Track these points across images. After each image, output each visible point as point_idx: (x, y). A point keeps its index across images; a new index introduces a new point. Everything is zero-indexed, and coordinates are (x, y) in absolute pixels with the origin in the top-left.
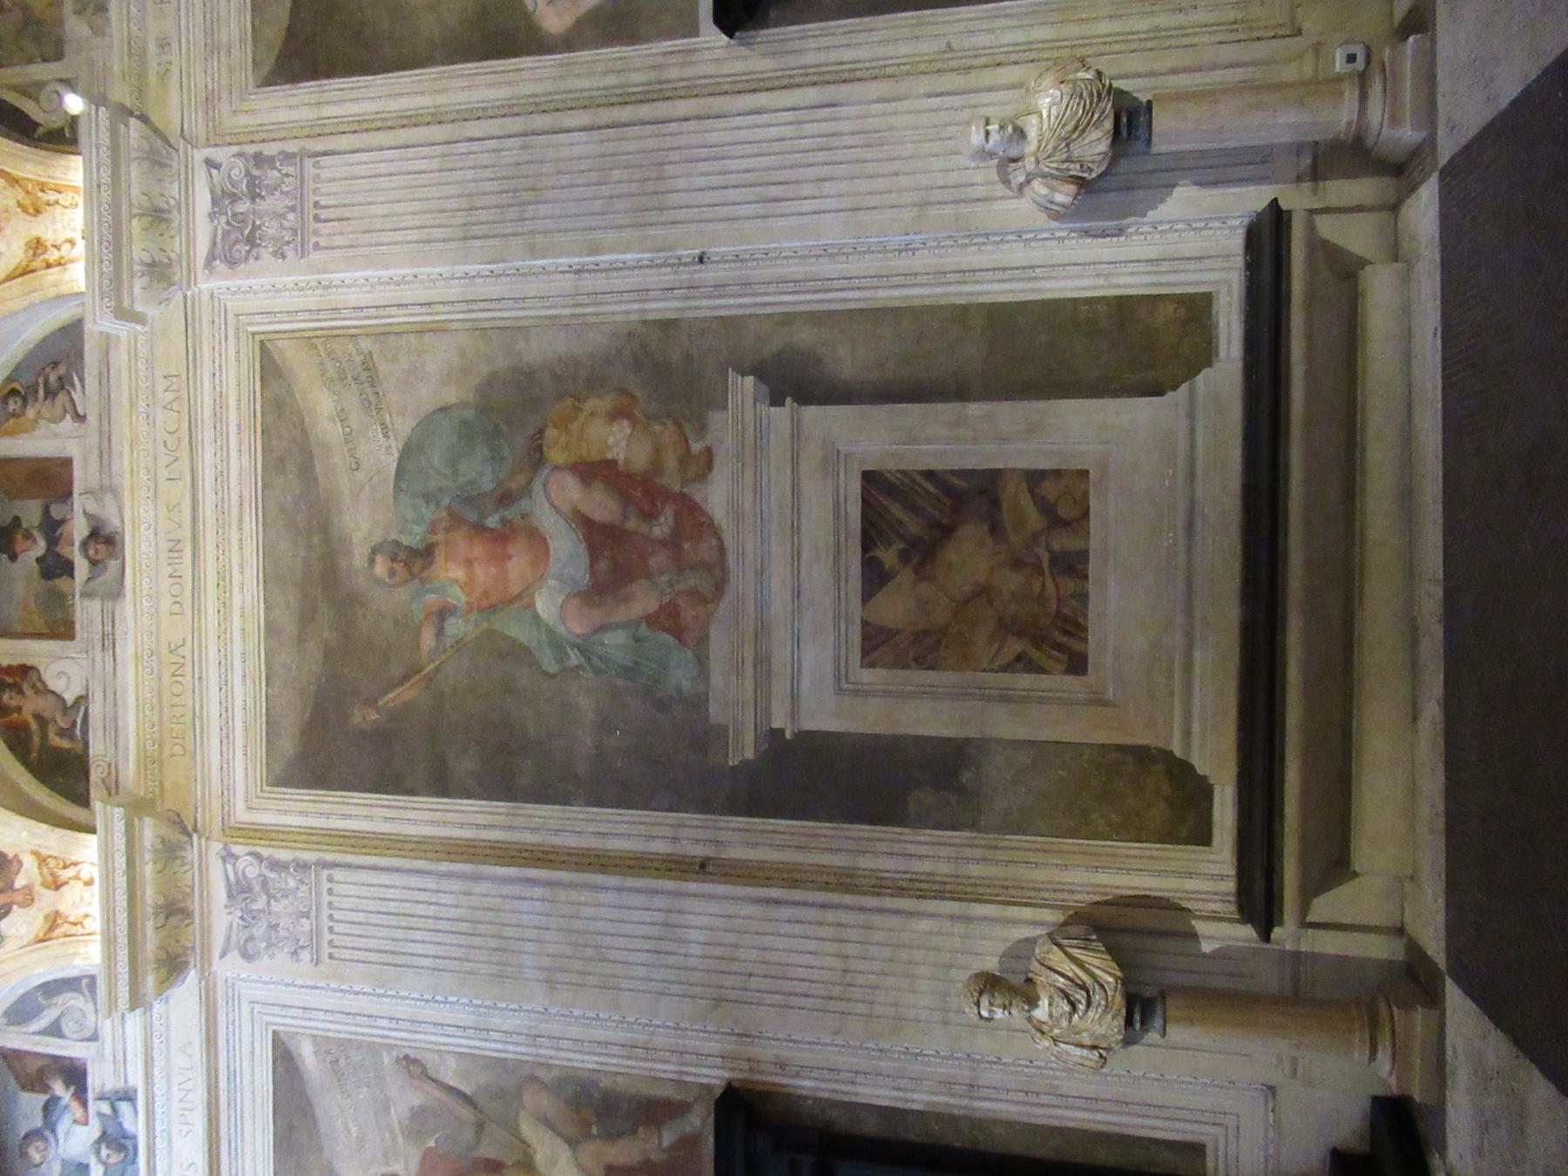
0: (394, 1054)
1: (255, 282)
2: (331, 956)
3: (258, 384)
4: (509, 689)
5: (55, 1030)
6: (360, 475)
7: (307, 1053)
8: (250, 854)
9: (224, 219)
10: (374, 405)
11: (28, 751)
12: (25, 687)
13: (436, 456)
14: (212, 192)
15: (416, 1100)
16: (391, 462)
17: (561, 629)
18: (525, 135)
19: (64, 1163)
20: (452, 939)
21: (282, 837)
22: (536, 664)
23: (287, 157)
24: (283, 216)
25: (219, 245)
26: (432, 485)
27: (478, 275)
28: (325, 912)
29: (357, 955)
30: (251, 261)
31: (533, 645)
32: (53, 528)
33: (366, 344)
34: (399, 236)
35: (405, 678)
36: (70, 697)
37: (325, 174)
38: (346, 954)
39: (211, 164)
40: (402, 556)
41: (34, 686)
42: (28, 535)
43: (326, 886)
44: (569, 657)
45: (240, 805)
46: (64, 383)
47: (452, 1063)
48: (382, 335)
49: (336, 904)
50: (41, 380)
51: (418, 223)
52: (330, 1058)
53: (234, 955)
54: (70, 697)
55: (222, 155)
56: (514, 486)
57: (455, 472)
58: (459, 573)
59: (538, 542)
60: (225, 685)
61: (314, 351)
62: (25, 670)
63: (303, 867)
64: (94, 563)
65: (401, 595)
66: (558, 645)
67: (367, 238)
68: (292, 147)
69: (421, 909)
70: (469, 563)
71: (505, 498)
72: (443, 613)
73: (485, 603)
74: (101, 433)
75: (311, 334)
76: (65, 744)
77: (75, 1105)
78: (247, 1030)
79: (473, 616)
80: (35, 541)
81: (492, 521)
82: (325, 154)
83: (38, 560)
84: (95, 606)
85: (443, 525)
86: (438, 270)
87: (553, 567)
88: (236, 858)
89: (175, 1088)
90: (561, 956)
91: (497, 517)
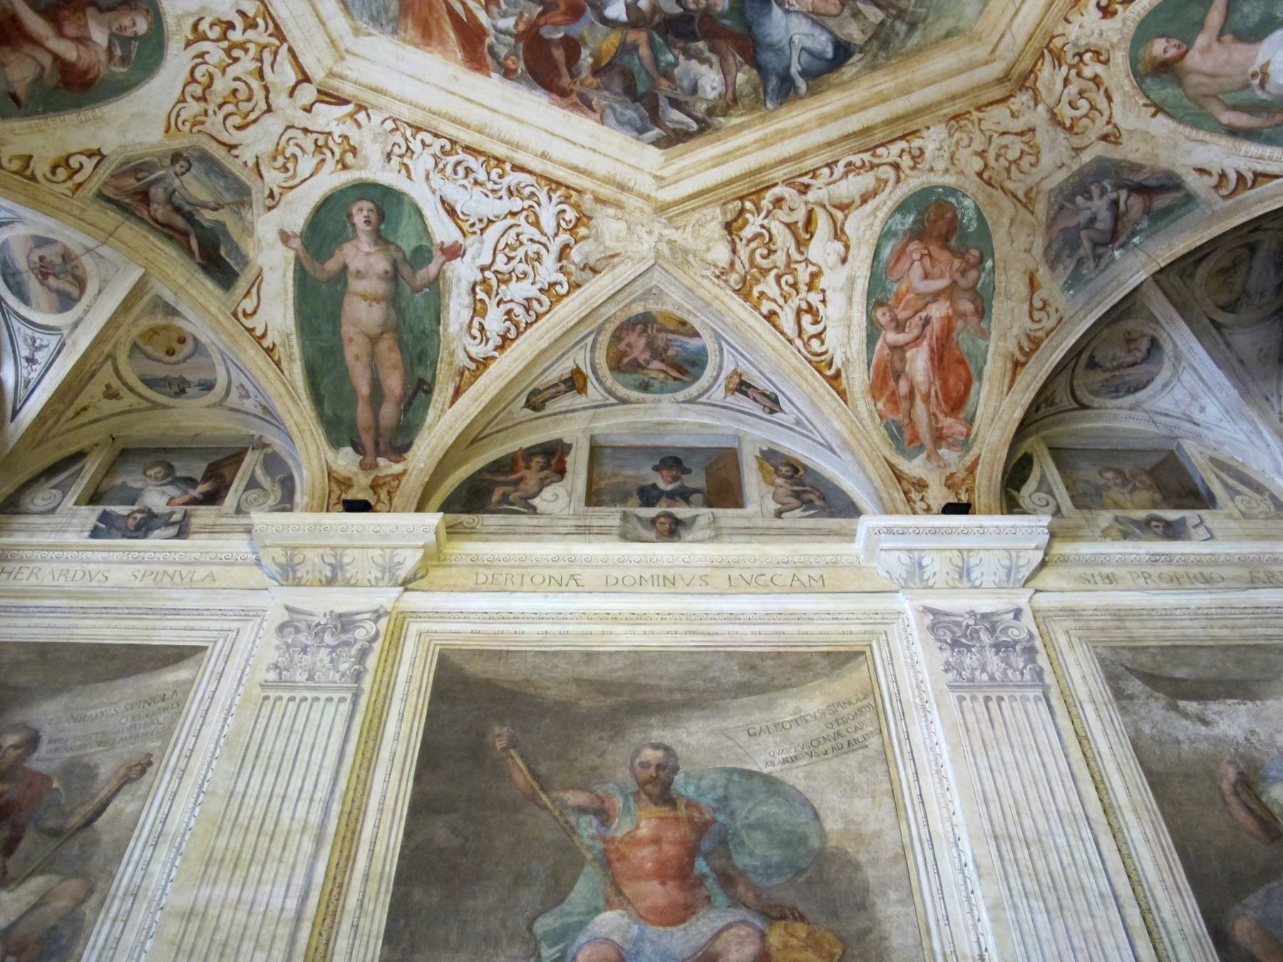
0: (157, 752)
1: (918, 647)
2: (266, 698)
3: (825, 649)
4: (520, 879)
5: (252, 484)
6: (743, 737)
7: (181, 674)
8: (377, 633)
9: (971, 622)
10: (813, 749)
11: (490, 472)
12: (546, 472)
13: (768, 809)
14: (992, 614)
15: (105, 772)
16: (759, 766)
17: (582, 939)
18: (1116, 898)
19: (141, 490)
20: (259, 811)
21: (390, 660)
22: (541, 913)
23: (1039, 673)
24: (984, 670)
25: (946, 619)
26: (737, 804)
27: (959, 852)
28: (310, 695)
29: (262, 722)
30: (939, 644)
31: (566, 907)
32: (684, 495)
33: (874, 742)
34: (985, 773)
35: (536, 776)
36: (536, 502)
37: (1031, 706)
38: (265, 712)
39: (1018, 613)
40: (662, 774)
41: (546, 478)
42: (675, 479)
43: (336, 696)
44: (550, 947)
45: (425, 626)
46: (809, 504)
47: (131, 808)
48: (885, 756)
49: (316, 704)
50: (808, 488)
51: (1002, 790)
52: (169, 693)
53: (286, 616)
54: (536, 502)
55: (1027, 619)
56: (741, 889)
57: (750, 827)
58: (644, 831)
59: (678, 915)
60: (539, 617)
61: (861, 696)
62: (561, 472)
63: (358, 677)
64: (653, 521)
65: (623, 774)
66: (565, 934)
67: (978, 743)
68: (1049, 678)
69: (296, 783)
70: (656, 841)
71: (727, 879)
72: (603, 814)
73: (613, 856)
74: (767, 528)
75: (877, 695)
77: (186, 498)
78: (218, 625)
79: (599, 845)
80: (670, 483)
81: (701, 865)
82: (1050, 707)
83: (654, 486)
84: (617, 522)
85: (696, 815)
86: (959, 812)
87: (652, 931)
88: (376, 621)
89: (178, 568)
90: (216, 928)
91: (706, 870)
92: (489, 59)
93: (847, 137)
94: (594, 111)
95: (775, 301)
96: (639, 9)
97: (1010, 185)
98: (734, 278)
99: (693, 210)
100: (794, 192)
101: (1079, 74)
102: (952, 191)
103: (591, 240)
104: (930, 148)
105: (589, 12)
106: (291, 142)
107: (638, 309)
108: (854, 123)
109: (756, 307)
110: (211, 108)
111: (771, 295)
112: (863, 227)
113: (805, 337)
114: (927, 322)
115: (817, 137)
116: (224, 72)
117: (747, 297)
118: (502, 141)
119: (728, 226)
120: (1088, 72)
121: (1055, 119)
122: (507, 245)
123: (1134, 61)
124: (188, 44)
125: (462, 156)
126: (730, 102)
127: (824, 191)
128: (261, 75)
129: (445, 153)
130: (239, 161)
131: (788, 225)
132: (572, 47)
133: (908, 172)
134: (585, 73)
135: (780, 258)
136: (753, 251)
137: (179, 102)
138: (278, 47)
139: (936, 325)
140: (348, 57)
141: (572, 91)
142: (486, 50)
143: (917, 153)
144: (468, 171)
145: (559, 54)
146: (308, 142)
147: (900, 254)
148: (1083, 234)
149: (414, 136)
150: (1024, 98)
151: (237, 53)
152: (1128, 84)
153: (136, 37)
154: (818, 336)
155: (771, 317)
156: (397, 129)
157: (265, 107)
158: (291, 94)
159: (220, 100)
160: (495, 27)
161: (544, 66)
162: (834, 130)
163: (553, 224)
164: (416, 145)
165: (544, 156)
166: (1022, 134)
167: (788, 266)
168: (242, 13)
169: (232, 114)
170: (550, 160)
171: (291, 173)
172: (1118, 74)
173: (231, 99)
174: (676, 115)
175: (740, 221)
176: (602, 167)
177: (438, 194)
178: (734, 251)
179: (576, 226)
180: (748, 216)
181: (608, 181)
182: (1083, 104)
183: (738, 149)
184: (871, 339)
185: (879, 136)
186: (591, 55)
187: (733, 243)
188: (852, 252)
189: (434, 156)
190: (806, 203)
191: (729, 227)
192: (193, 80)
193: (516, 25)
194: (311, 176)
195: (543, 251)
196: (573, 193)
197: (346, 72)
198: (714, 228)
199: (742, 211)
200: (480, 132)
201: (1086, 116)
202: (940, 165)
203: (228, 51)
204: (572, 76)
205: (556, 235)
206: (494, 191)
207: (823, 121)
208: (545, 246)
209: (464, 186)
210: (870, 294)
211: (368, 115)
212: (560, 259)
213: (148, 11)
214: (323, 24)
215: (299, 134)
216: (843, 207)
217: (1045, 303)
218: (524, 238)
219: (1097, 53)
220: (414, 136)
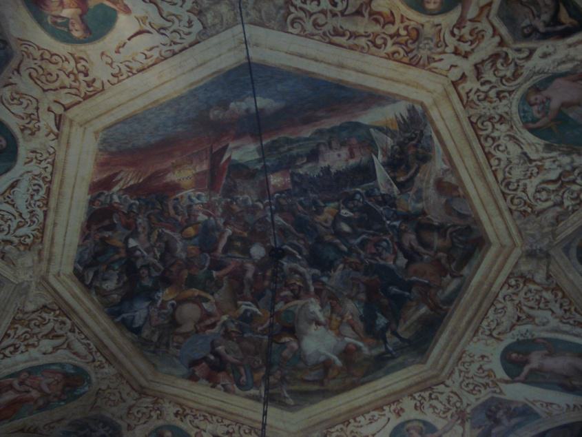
92: (97, 193)
93: (101, 341)
94: (85, 239)
95: (15, 334)
96: (135, 251)
97: (99, 400)
98: (20, 315)
99: (48, 291)
100: (70, 327)
101: (151, 411)
102: (90, 382)
103: (18, 252)
104: (106, 370)
105: (130, 232)
106: (29, 102)
108: (107, 341)
109: (9, 328)
110: (39, 63)
111: (18, 332)
112: (63, 356)
113: (3, 351)
114: (28, 392)
115: (97, 329)
116: (60, 70)
117: (12, 323)
118: (57, 205)
119: (45, 307)
120: (152, 414)
121: (130, 408)
122: (3, 215)
123: (161, 427)
124: (72, 55)
125: (44, 187)
126: (103, 294)
127: (73, 338)
128: (65, 87)
129: (44, 179)
130: (11, 75)
131: (53, 329)
132: (112, 227)
133: (93, 365)
134: (100, 235)
135: (37, 330)
136: (37, 319)
137: (38, 47)
138: (79, 96)
139: (28, 396)
140: (82, 129)
141: (90, 231)
142: (101, 191)
143: (102, 366)
144: (37, 191)
145: (107, 222)
146: (30, 111)
147: (54, 372)
148: (88, 430)
149: (48, 163)
150: (137, 395)
151: (72, 77)
152: (152, 427)
153: (69, 30)
154: (5, 356)
155: (7, 335)
156: (50, 154)
157: (46, 88)
158: (55, 101)
159: (44, 66)
160: (113, 194)
161: (99, 217)
162: (102, 335)
163: (21, 234)
164: (44, 164)
165: (55, 224)
166: (122, 398)
167: (34, 334)
168: (94, 80)
169: (37, 71)
170: (54, 227)
171: (10, 101)
172: (156, 423)
173: (45, 73)
174: (91, 275)
175: (49, 311)
176: (57, 250)
177: (21, 178)
178: (34, 312)
179: (23, 244)
180: (52, 313)
181: (51, 254)
182: (140, 415)
183: (82, 302)
184: (12, 376)
186: (109, 236)
187: (38, 310)
188: (50, 356)
189: (41, 174)
190: (66, 333)
191: (44, 308)
192: (52, 55)
193: (116, 203)
194: (13, 113)
195: (5, 233)
196: (40, 240)
197: (74, 129)
198: (42, 301)
199: (54, 310)
200: (60, 194)
201: (135, 417)
202: (99, 376)
203: (72, 73)
204: (98, 230)
205: (16, 237)
206: (30, 204)
207: (105, 330)
208: (8, 233)
209: (28, 190)
210: (32, 368)
211: (53, 140)
212: (3, 241)
213: (85, 38)
214: (96, 118)
215: (35, 105)
216: (69, 347)
217: (53, 428)
218: (9, 222)
219: (160, 415)
220: (48, 163)
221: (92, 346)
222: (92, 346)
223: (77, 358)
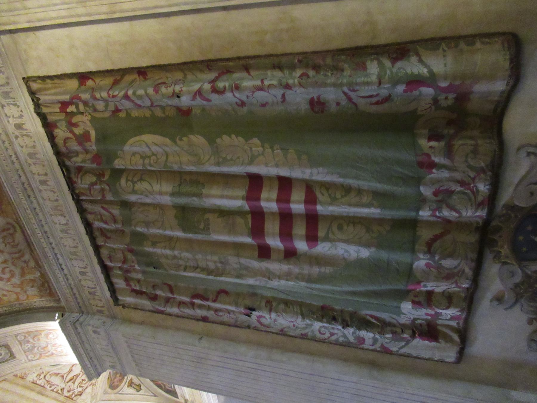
76: (170, 389)
104: (35, 375)
107: (109, 391)
119: (80, 395)
131: (74, 383)
143: (38, 376)
178: (87, 388)
185: (39, 388)
216: (63, 377)
221: (48, 387)
222: (48, 387)
223: (55, 372)
